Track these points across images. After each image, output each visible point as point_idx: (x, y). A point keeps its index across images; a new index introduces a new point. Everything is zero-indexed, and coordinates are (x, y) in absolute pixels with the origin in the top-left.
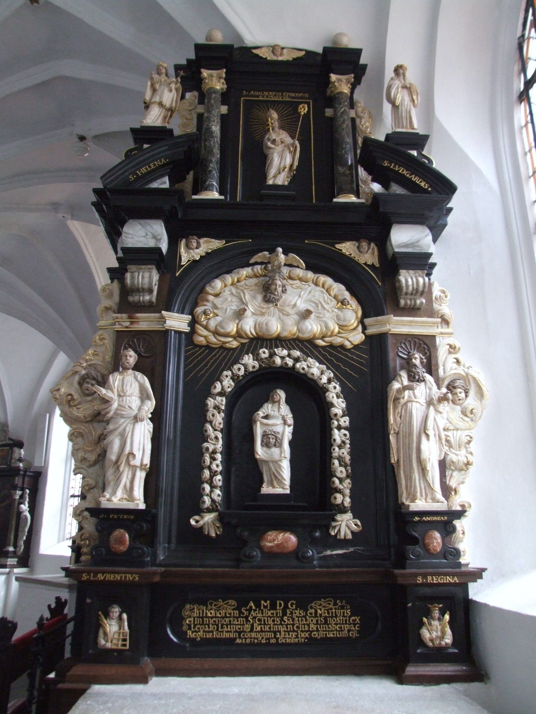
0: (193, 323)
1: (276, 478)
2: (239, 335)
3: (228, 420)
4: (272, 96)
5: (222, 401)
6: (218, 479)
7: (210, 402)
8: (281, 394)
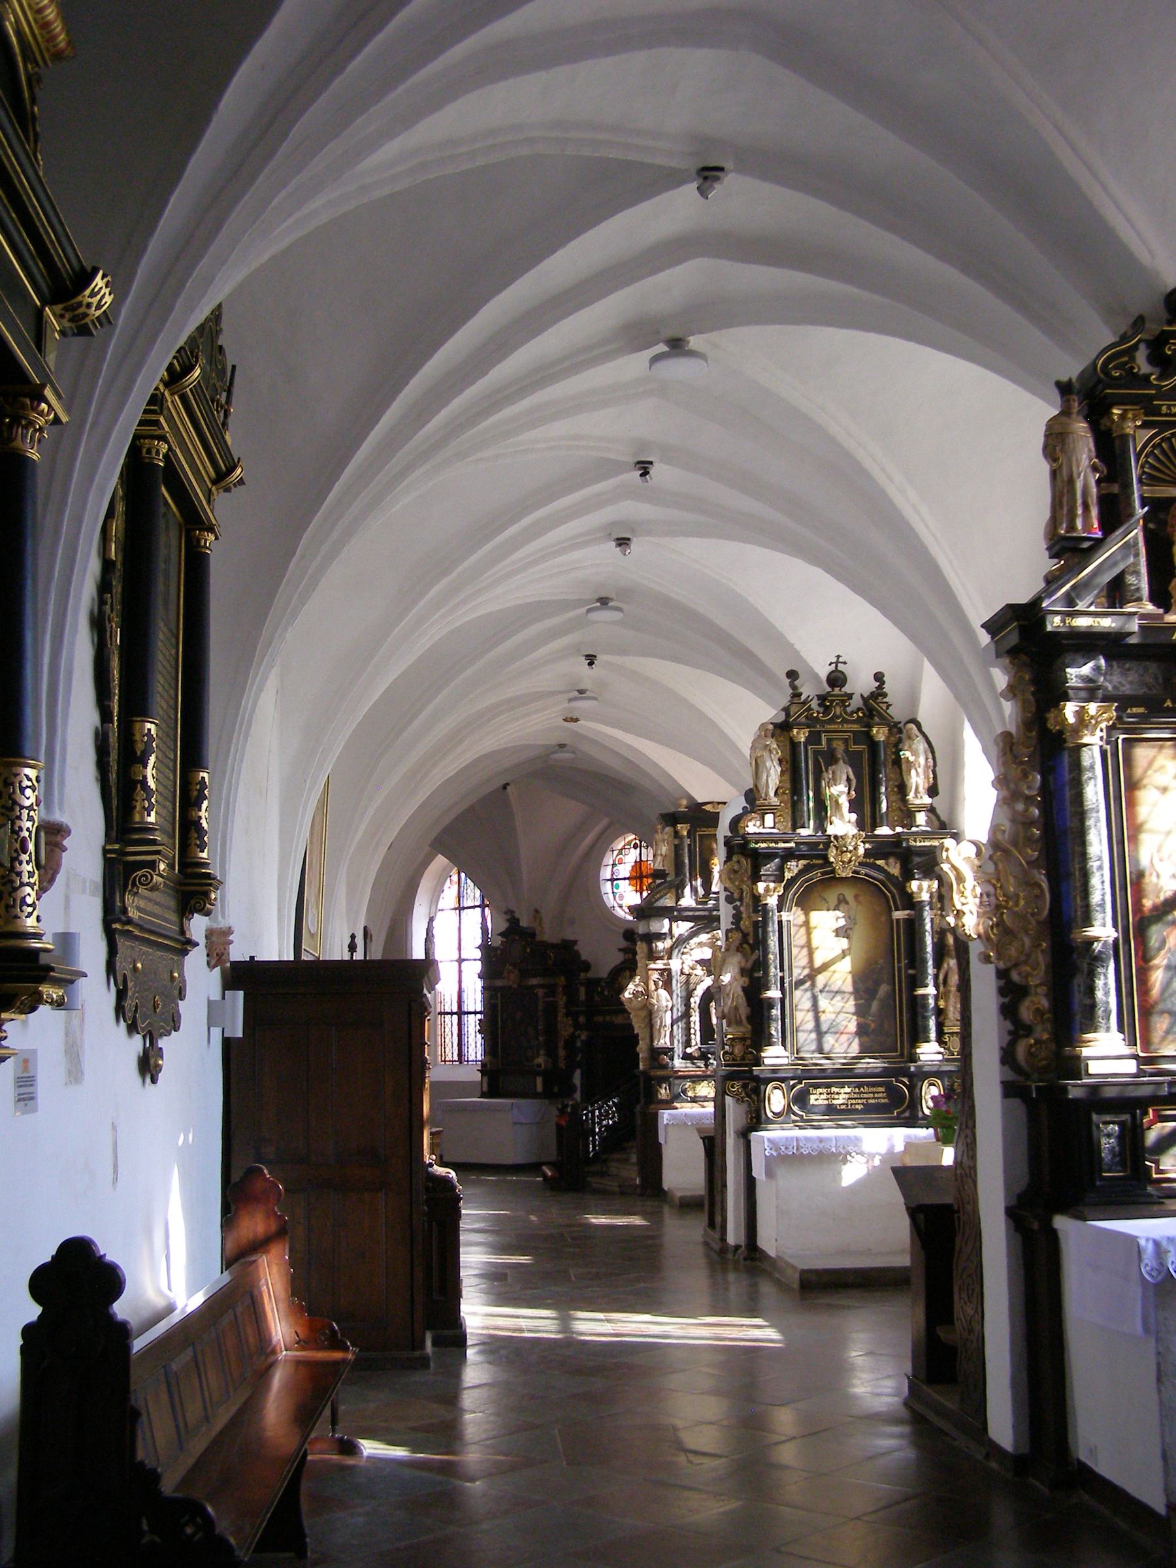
6: (698, 1033)
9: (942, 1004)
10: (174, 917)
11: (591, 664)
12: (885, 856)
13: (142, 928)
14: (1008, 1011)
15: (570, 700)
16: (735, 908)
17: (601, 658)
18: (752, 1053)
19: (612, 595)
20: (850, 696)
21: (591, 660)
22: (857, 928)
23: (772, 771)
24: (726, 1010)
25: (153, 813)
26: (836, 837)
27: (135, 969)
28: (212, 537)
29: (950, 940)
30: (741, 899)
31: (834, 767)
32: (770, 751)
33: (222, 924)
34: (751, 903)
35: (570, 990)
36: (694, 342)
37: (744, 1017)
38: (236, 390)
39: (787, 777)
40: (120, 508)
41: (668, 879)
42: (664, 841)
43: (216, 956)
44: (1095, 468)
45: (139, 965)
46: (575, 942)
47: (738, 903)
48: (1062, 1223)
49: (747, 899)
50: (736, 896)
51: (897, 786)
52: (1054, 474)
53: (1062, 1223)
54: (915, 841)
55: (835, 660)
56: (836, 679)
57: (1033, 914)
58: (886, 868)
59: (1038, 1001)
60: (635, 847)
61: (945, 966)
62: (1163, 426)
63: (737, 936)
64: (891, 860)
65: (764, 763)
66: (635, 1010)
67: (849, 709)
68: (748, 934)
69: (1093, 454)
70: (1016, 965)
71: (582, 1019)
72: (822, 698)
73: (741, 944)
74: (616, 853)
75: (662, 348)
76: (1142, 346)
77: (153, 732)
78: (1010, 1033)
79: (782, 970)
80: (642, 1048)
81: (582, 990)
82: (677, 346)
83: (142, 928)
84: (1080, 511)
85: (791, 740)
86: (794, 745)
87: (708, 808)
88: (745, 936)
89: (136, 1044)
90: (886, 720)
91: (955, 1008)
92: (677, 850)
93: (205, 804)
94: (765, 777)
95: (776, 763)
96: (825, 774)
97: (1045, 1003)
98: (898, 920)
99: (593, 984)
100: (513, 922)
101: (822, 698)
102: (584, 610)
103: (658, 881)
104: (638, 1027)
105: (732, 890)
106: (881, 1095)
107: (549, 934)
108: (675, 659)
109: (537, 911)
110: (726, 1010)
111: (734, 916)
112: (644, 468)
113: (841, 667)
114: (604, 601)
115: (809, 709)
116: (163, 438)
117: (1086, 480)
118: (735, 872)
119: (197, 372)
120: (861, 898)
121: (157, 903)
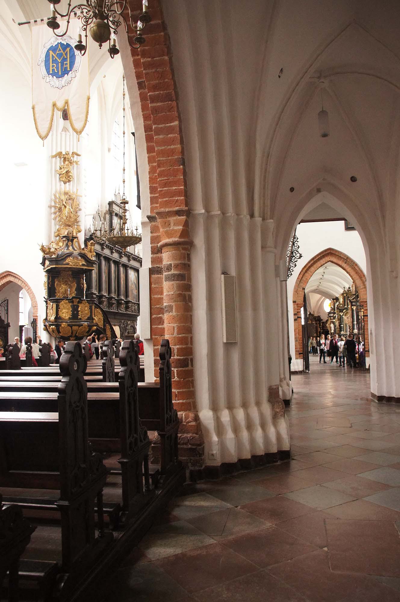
46: (320, 316)
59: (351, 328)
63: (338, 319)
71: (321, 328)
72: (348, 290)
80: (329, 332)
81: (321, 324)
86: (344, 296)
99: (323, 323)
101: (348, 290)
104: (329, 329)
107: (316, 315)
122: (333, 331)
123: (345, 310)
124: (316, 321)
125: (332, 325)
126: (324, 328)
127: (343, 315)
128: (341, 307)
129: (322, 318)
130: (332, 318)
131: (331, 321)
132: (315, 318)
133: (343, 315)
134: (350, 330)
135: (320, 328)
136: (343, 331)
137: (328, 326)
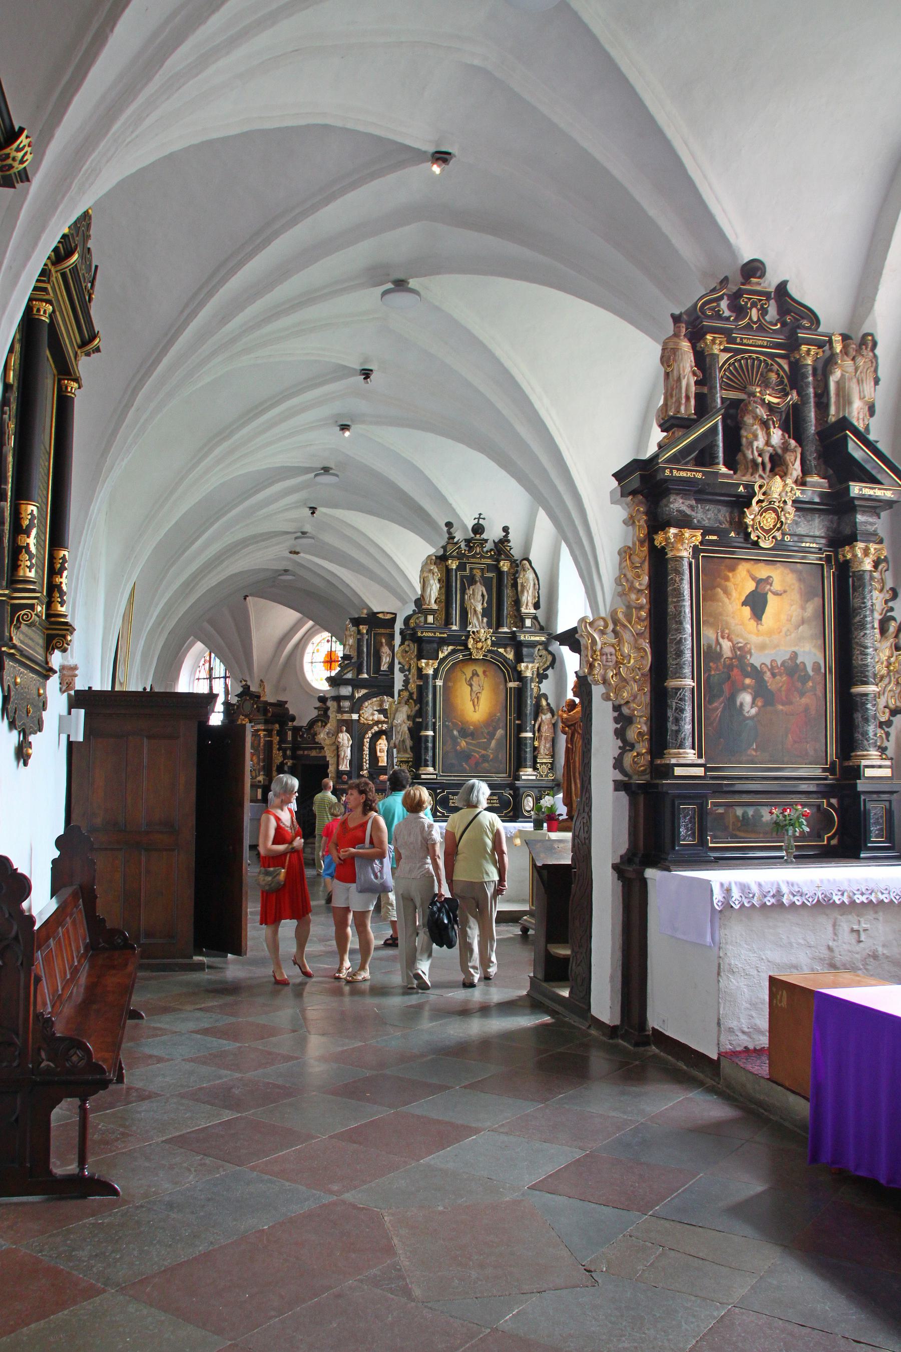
0: (359, 717)
1: (383, 761)
2: (373, 720)
3: (370, 745)
4: (382, 631)
5: (368, 740)
6: (368, 762)
7: (365, 740)
8: (384, 737)
9: (536, 744)
10: (41, 651)
11: (313, 513)
12: (505, 646)
13: (22, 655)
14: (620, 734)
15: (296, 538)
16: (405, 676)
17: (321, 510)
18: (412, 771)
19: (332, 466)
20: (486, 541)
21: (313, 510)
22: (484, 692)
23: (434, 587)
24: (397, 743)
25: (33, 570)
26: (473, 632)
27: (16, 684)
28: (76, 385)
29: (544, 703)
30: (409, 670)
31: (473, 587)
32: (433, 574)
33: (71, 662)
34: (416, 673)
35: (282, 734)
36: (413, 283)
37: (408, 747)
38: (97, 283)
39: (443, 590)
40: (17, 347)
41: (353, 661)
42: (351, 635)
43: (66, 685)
44: (694, 374)
45: (18, 680)
46: (286, 702)
47: (407, 673)
48: (651, 873)
49: (414, 671)
50: (406, 667)
51: (513, 601)
52: (667, 375)
53: (651, 873)
54: (525, 637)
55: (478, 516)
56: (478, 529)
57: (639, 669)
58: (504, 654)
59: (641, 726)
60: (328, 641)
61: (540, 719)
62: (737, 352)
63: (405, 694)
64: (508, 649)
65: (429, 581)
66: (327, 745)
67: (485, 550)
68: (413, 693)
69: (693, 364)
70: (627, 702)
71: (288, 752)
72: (468, 541)
73: (408, 700)
74: (315, 645)
75: (390, 286)
76: (725, 297)
77: (35, 513)
78: (620, 748)
79: (435, 717)
80: (331, 769)
81: (290, 733)
82: (400, 285)
83: (22, 655)
84: (683, 401)
85: (447, 567)
86: (448, 571)
87: (380, 616)
88: (411, 694)
89: (14, 738)
90: (509, 557)
91: (545, 747)
92: (359, 642)
93: (65, 573)
94: (429, 591)
95: (436, 581)
96: (467, 591)
97: (645, 729)
98: (511, 688)
99: (296, 730)
100: (246, 688)
102: (312, 475)
103: (346, 662)
105: (404, 663)
106: (495, 801)
107: (269, 697)
108: (371, 512)
109: (261, 681)
110: (397, 743)
111: (404, 681)
112: (367, 374)
113: (481, 521)
114: (326, 470)
115: (460, 547)
116: (49, 302)
117: (688, 381)
118: (407, 652)
119: (76, 257)
120: (487, 673)
121: (31, 639)
122: (345, 766)
123: (447, 650)
124: (266, 722)
125: (345, 739)
126: (300, 752)
127: (435, 676)
128: (430, 629)
129: (291, 712)
130: (346, 704)
131: (339, 716)
132: (265, 712)
133: (435, 676)
134: (627, 746)
135: (284, 750)
136: (434, 766)
137: (328, 742)
